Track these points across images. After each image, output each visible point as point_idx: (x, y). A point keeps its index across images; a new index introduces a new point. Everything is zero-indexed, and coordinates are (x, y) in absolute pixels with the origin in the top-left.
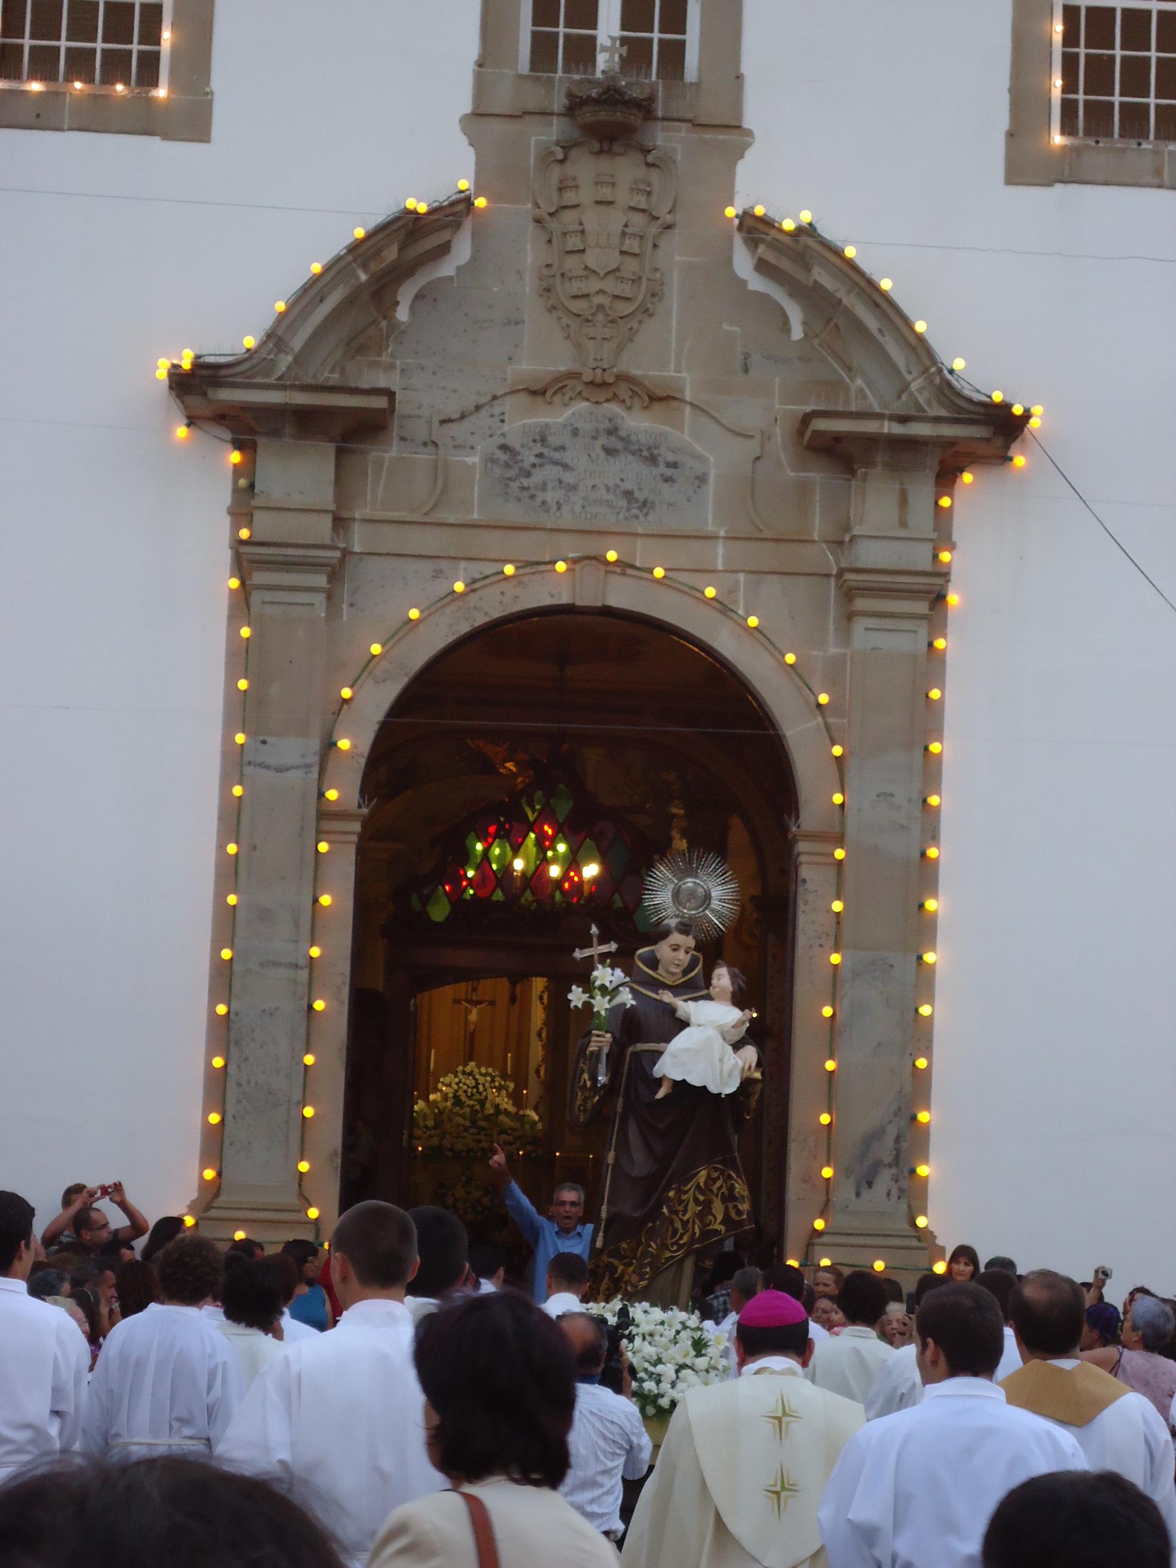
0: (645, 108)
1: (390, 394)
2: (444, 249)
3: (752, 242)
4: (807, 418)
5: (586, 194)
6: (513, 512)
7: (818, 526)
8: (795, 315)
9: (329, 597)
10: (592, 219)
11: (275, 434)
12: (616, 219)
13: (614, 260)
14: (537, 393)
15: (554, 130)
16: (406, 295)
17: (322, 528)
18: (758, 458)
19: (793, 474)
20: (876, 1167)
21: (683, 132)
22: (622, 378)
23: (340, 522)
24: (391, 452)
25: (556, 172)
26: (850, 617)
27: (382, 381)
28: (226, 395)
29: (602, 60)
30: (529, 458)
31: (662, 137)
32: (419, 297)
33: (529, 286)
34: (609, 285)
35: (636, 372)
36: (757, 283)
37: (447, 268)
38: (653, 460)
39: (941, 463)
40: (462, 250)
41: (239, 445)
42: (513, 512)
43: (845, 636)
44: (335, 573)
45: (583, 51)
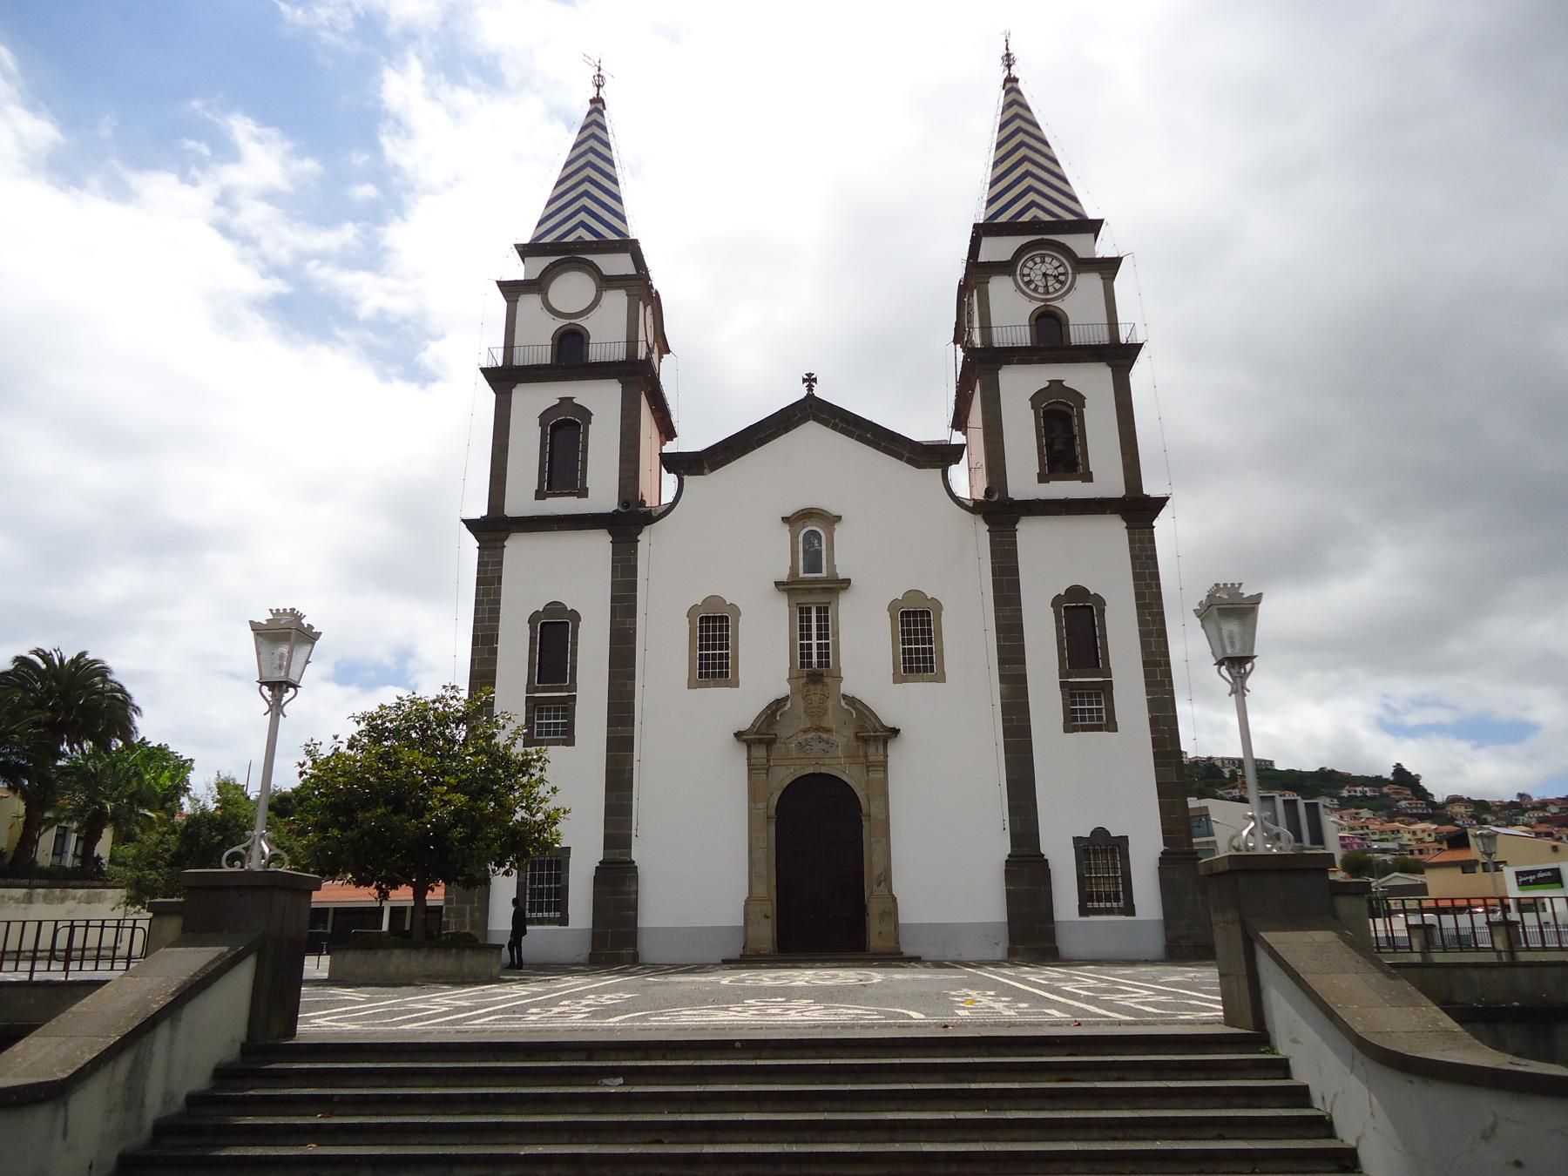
0: (822, 675)
1: (776, 735)
2: (785, 705)
3: (844, 699)
4: (857, 733)
5: (812, 692)
6: (802, 755)
7: (861, 753)
8: (854, 713)
9: (767, 775)
10: (813, 697)
11: (754, 744)
12: (818, 696)
13: (818, 705)
14: (805, 731)
15: (805, 680)
16: (778, 714)
17: (765, 761)
18: (848, 741)
19: (855, 744)
20: (881, 881)
21: (830, 679)
22: (821, 727)
23: (768, 761)
24: (778, 745)
25: (806, 689)
26: (868, 771)
27: (772, 732)
28: (743, 737)
29: (815, 666)
30: (804, 744)
31: (828, 680)
32: (781, 714)
33: (802, 710)
34: (818, 709)
35: (824, 726)
36: (846, 707)
37: (786, 708)
38: (828, 743)
39: (884, 740)
40: (789, 705)
41: (749, 747)
42: (802, 755)
43: (868, 775)
44: (767, 770)
45: (810, 664)
